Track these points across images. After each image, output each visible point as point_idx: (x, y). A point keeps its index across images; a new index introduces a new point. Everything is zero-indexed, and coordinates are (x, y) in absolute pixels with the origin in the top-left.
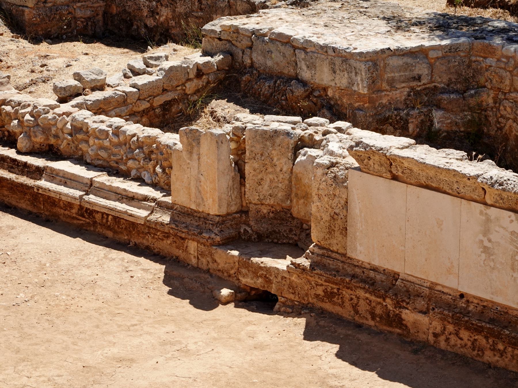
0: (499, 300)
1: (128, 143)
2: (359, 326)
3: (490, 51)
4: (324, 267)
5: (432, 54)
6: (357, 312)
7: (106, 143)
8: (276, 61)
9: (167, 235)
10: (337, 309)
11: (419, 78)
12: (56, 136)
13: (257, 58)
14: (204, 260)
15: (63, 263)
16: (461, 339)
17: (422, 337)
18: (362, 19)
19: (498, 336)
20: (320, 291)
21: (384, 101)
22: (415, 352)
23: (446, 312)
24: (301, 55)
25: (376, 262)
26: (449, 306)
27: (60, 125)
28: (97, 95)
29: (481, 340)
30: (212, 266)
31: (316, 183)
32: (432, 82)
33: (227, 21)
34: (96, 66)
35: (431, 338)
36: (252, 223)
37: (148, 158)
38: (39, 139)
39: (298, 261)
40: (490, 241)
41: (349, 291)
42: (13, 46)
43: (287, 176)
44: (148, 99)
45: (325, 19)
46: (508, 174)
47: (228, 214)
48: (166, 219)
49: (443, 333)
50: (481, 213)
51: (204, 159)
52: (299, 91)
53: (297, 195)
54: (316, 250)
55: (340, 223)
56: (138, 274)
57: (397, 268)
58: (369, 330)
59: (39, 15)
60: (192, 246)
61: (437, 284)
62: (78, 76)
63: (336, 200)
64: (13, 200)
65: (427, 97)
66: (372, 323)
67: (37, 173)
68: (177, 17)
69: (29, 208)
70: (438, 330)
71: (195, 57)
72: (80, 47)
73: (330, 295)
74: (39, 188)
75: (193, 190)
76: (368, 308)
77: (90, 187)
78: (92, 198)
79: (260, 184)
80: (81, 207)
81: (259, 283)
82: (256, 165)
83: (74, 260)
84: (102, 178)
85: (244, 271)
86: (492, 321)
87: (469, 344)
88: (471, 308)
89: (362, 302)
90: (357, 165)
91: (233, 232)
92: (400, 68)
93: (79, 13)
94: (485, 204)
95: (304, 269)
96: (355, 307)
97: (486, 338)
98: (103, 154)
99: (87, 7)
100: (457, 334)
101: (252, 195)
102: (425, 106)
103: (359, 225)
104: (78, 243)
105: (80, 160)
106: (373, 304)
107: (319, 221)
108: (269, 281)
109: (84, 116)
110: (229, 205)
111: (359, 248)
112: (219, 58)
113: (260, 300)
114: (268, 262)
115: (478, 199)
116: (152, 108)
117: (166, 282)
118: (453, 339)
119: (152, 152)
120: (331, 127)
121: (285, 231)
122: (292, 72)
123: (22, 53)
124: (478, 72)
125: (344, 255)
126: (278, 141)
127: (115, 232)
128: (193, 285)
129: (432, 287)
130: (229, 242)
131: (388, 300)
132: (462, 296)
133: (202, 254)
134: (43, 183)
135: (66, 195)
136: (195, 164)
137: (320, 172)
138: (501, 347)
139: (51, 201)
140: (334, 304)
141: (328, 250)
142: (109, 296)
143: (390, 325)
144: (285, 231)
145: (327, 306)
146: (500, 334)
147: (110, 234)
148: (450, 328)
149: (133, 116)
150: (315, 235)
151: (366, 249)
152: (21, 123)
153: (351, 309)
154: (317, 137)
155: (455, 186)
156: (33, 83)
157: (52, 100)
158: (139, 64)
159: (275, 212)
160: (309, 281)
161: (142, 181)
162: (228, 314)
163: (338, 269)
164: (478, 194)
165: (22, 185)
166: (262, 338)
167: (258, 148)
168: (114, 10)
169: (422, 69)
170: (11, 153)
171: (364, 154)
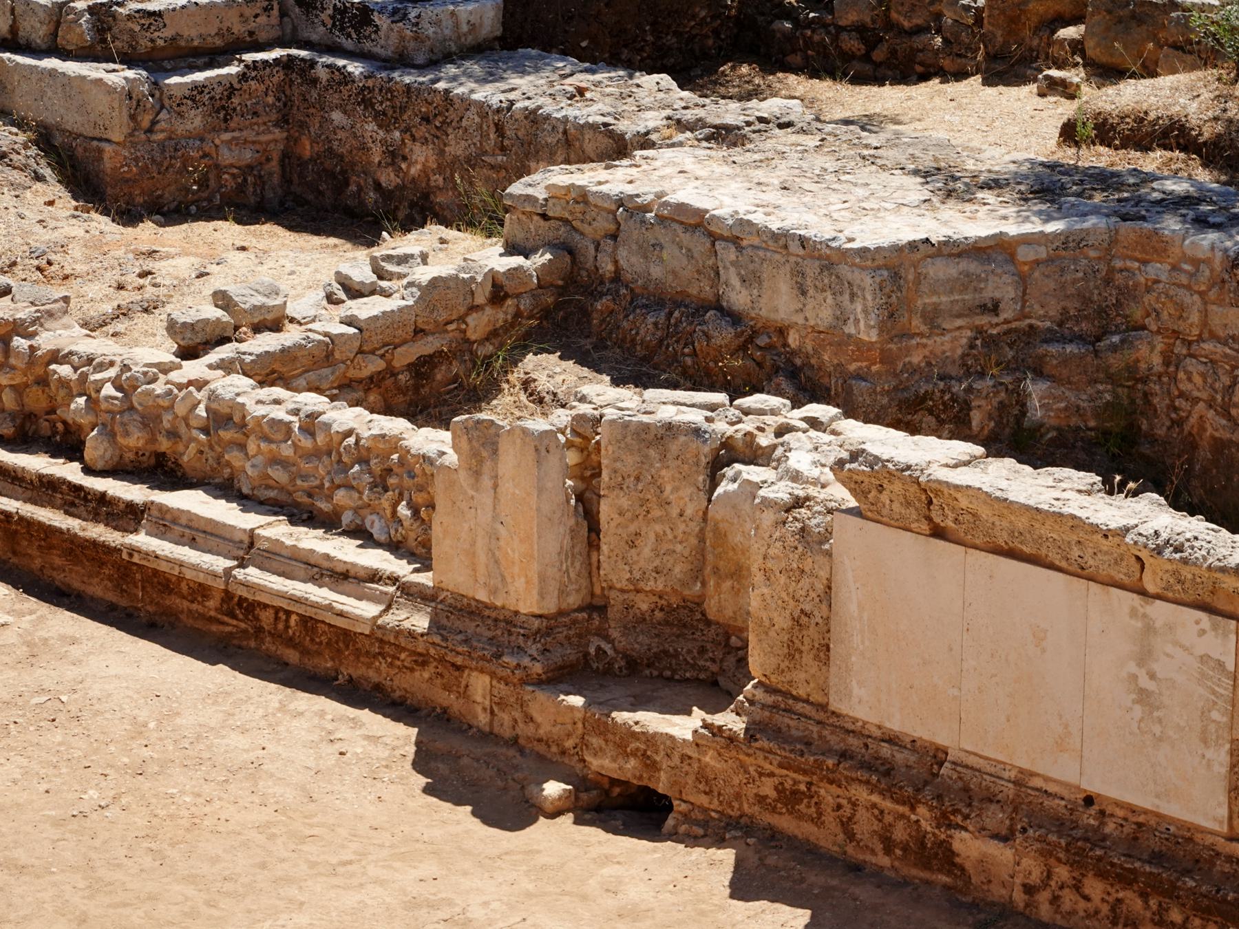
0: (1173, 809)
2: (856, 868)
3: (1156, 247)
4: (777, 734)
5: (1025, 254)
6: (851, 836)
7: (286, 450)
8: (670, 267)
9: (422, 660)
10: (804, 830)
11: (994, 308)
12: (173, 434)
13: (630, 260)
14: (505, 717)
15: (187, 721)
16: (1087, 898)
17: (998, 892)
18: (866, 173)
19: (1171, 892)
20: (767, 788)
21: (916, 359)
23: (1053, 838)
24: (728, 254)
25: (895, 724)
26: (1060, 824)
27: (181, 410)
28: (267, 342)
30: (524, 730)
31: (759, 544)
32: (1023, 316)
33: (560, 176)
34: (265, 275)
35: (1019, 897)
36: (615, 634)
37: (380, 484)
38: (135, 439)
39: (720, 719)
40: (1152, 676)
41: (834, 789)
42: (75, 229)
43: (695, 527)
44: (382, 351)
45: (782, 172)
46: (1195, 527)
47: (561, 613)
48: (420, 622)
49: (1045, 884)
50: (1133, 613)
51: (507, 487)
52: (724, 335)
53: (716, 570)
54: (760, 695)
55: (813, 634)
56: (358, 748)
57: (942, 738)
58: (877, 877)
59: (136, 160)
60: (479, 684)
61: (1033, 774)
62: (222, 299)
63: (805, 582)
64: (74, 578)
65: (1013, 349)
66: (885, 861)
67: (131, 516)
68: (447, 166)
69: (111, 597)
70: (1035, 877)
71: (486, 256)
72: (227, 232)
73: (789, 798)
74: (133, 550)
75: (482, 558)
76: (876, 826)
77: (248, 549)
79: (632, 545)
80: (228, 595)
81: (629, 769)
82: (624, 502)
83: (211, 716)
84: (276, 530)
85: (595, 741)
86: (1157, 858)
87: (1105, 909)
88: (1110, 828)
89: (862, 815)
90: (852, 503)
91: (571, 654)
92: (954, 285)
93: (227, 156)
94: (1143, 593)
95: (732, 739)
96: (846, 825)
97: (1144, 895)
99: (246, 141)
100: (1077, 888)
101: (614, 572)
102: (1008, 368)
103: (857, 639)
104: (221, 675)
105: (226, 489)
106: (888, 819)
109: (236, 387)
110: (562, 592)
111: (857, 691)
112: (542, 258)
113: (633, 807)
114: (651, 721)
115: (1126, 580)
116: (391, 372)
117: (420, 765)
118: (1069, 899)
119: (389, 471)
120: (795, 416)
121: (687, 651)
122: (708, 292)
123: (97, 246)
125: (823, 707)
126: (674, 448)
127: (305, 652)
128: (481, 773)
130: (563, 676)
131: (922, 810)
132: (1089, 800)
133: (502, 704)
134: (142, 540)
135: (196, 568)
136: (486, 499)
137: (768, 517)
139: (162, 580)
140: (801, 817)
141: (786, 694)
142: (290, 795)
143: (927, 866)
144: (687, 651)
145: (785, 823)
146: (1174, 886)
147: (292, 656)
148: (1063, 873)
149: (347, 390)
151: (873, 693)
152: (92, 403)
153: (838, 830)
154: (764, 440)
155: (1076, 552)
156: (122, 313)
157: (165, 352)
158: (361, 272)
159: (668, 610)
160: (743, 766)
162: (560, 842)
163: (807, 737)
164: (1125, 569)
165: (94, 544)
166: (636, 892)
167: (630, 463)
168: (307, 149)
169: (1002, 287)
170: (71, 472)
171: (869, 480)
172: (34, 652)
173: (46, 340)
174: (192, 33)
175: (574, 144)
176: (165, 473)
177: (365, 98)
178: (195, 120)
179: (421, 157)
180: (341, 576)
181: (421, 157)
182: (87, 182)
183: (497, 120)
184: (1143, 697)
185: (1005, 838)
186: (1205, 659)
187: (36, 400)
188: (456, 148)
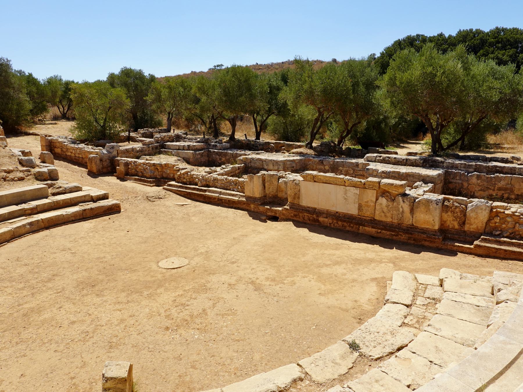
0: (350, 212)
1: (230, 182)
2: (305, 223)
4: (293, 208)
5: (297, 161)
9: (244, 204)
10: (298, 219)
11: (293, 167)
15: (217, 212)
19: (351, 222)
20: (292, 215)
22: (325, 229)
25: (309, 206)
29: (345, 224)
30: (258, 211)
35: (328, 225)
38: (204, 183)
39: (285, 207)
51: (255, 182)
55: (297, 195)
56: (238, 214)
57: (316, 207)
58: (308, 224)
60: (252, 206)
73: (295, 216)
77: (220, 193)
78: (222, 196)
81: (273, 214)
83: (219, 212)
86: (348, 218)
91: (263, 202)
93: (203, 160)
94: (345, 186)
95: (287, 209)
96: (304, 218)
98: (223, 185)
100: (337, 223)
105: (216, 187)
107: (290, 196)
108: (276, 213)
112: (243, 165)
113: (275, 219)
118: (336, 224)
119: (236, 183)
121: (277, 200)
122: (262, 167)
124: (307, 165)
128: (256, 215)
129: (327, 211)
130: (264, 204)
134: (207, 193)
136: (252, 184)
137: (291, 182)
138: (352, 225)
143: (315, 222)
145: (295, 219)
147: (227, 205)
148: (335, 221)
150: (289, 200)
151: (305, 202)
152: (199, 179)
161: (233, 191)
164: (344, 183)
165: (201, 194)
166: (279, 228)
167: (269, 179)
168: (210, 159)
169: (294, 165)
170: (197, 187)
172: (195, 207)
173: (192, 173)
174: (198, 147)
175: (241, 155)
176: (209, 187)
177: (217, 153)
178: (199, 156)
179: (223, 159)
180: (233, 195)
181: (223, 159)
182: (188, 162)
183: (232, 154)
184: (345, 199)
185: (326, 218)
186: (354, 193)
187: (191, 180)
188: (227, 158)
